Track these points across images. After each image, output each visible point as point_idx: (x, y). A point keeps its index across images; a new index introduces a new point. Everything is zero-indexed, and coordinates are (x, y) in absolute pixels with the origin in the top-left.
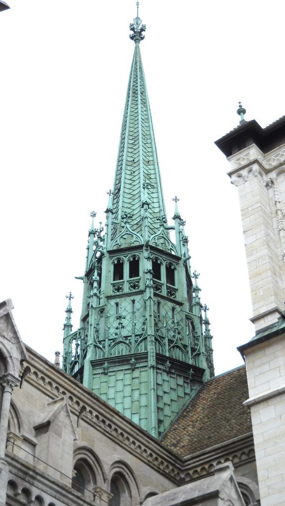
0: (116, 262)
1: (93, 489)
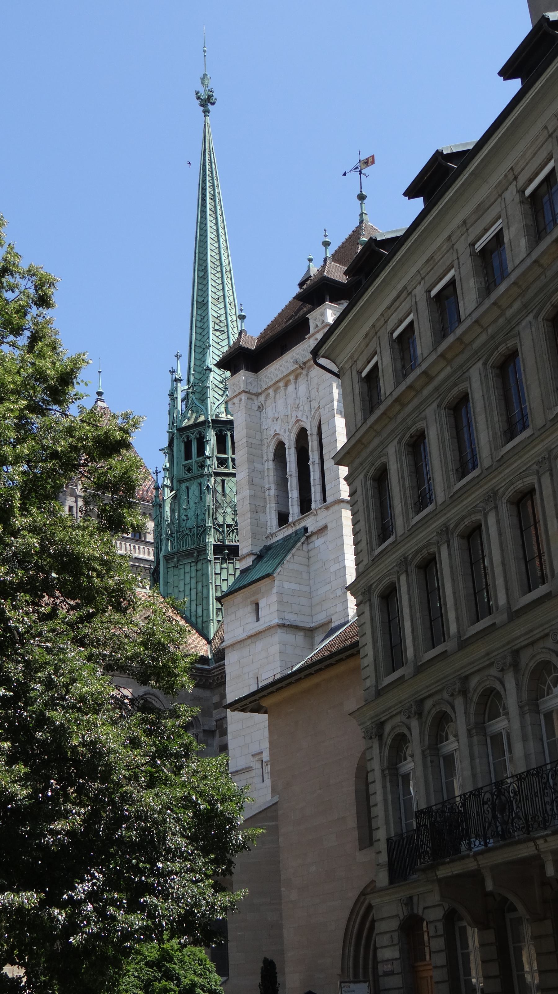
0: (186, 440)
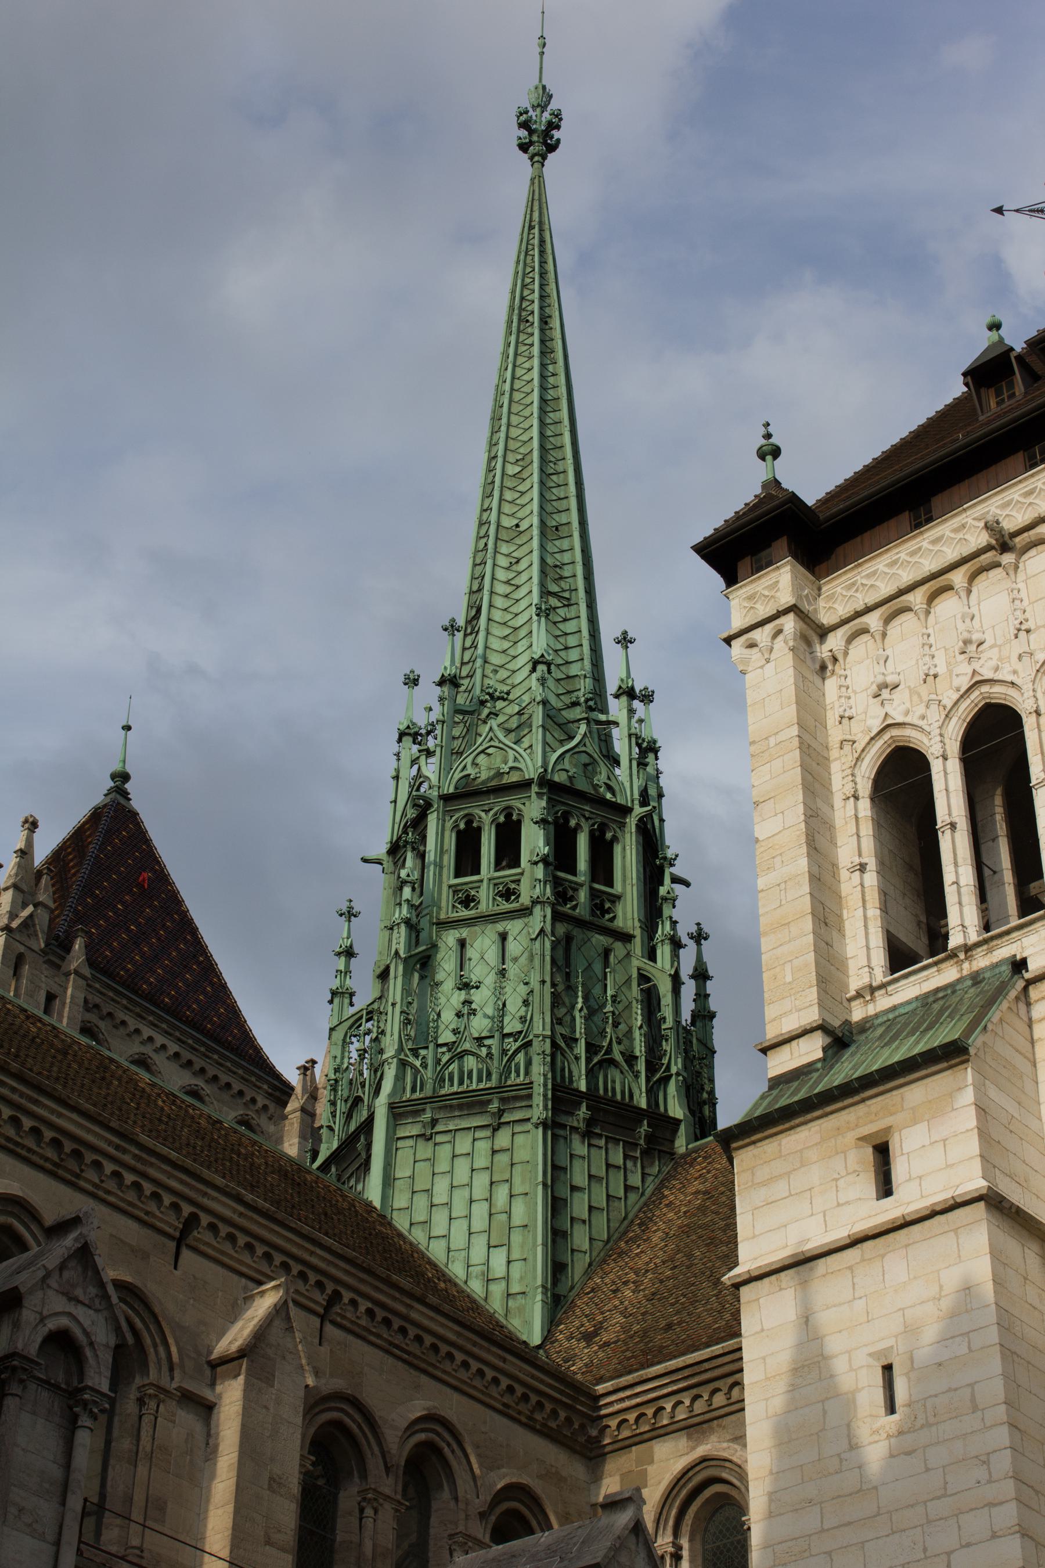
0: (462, 826)
1: (358, 1492)
